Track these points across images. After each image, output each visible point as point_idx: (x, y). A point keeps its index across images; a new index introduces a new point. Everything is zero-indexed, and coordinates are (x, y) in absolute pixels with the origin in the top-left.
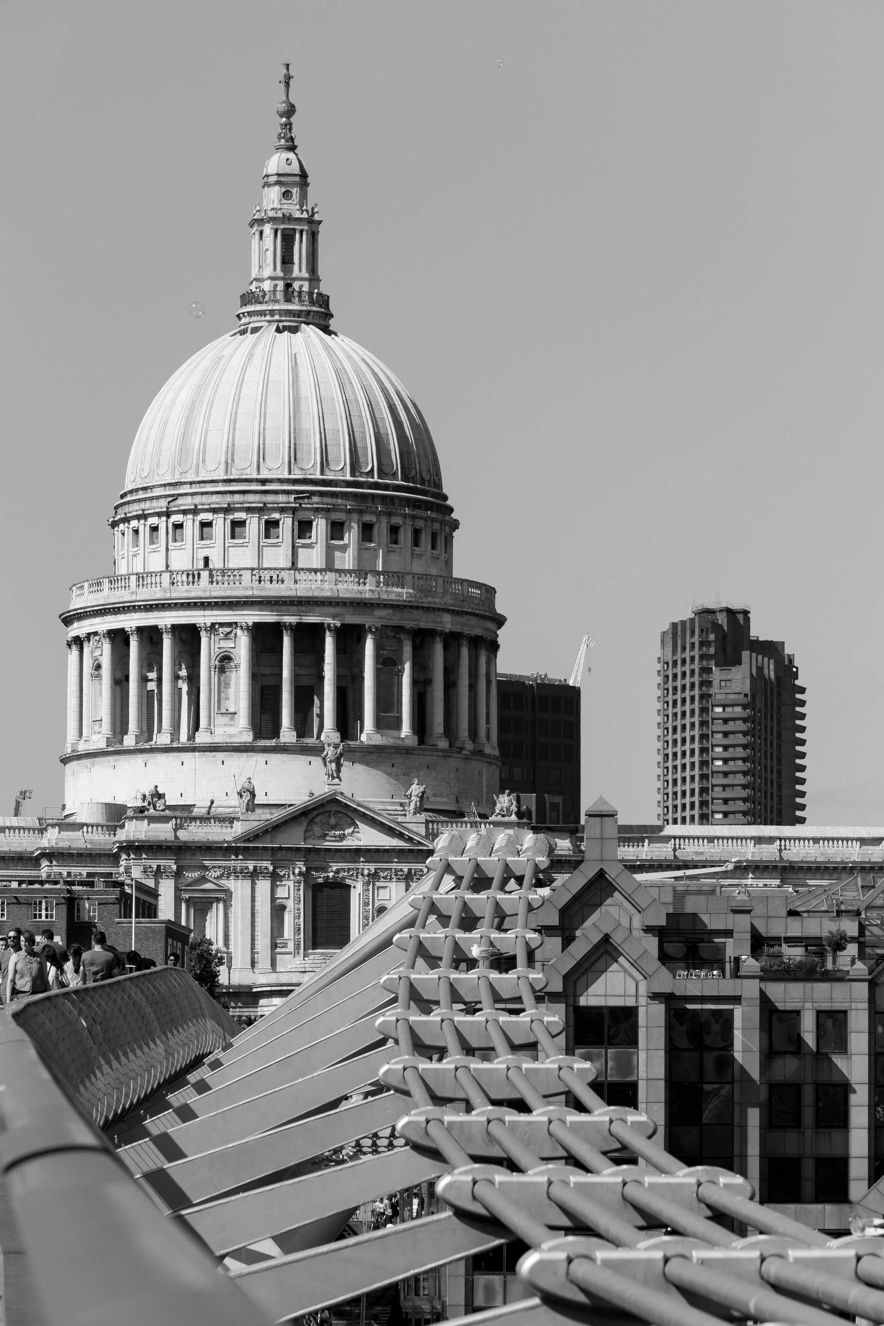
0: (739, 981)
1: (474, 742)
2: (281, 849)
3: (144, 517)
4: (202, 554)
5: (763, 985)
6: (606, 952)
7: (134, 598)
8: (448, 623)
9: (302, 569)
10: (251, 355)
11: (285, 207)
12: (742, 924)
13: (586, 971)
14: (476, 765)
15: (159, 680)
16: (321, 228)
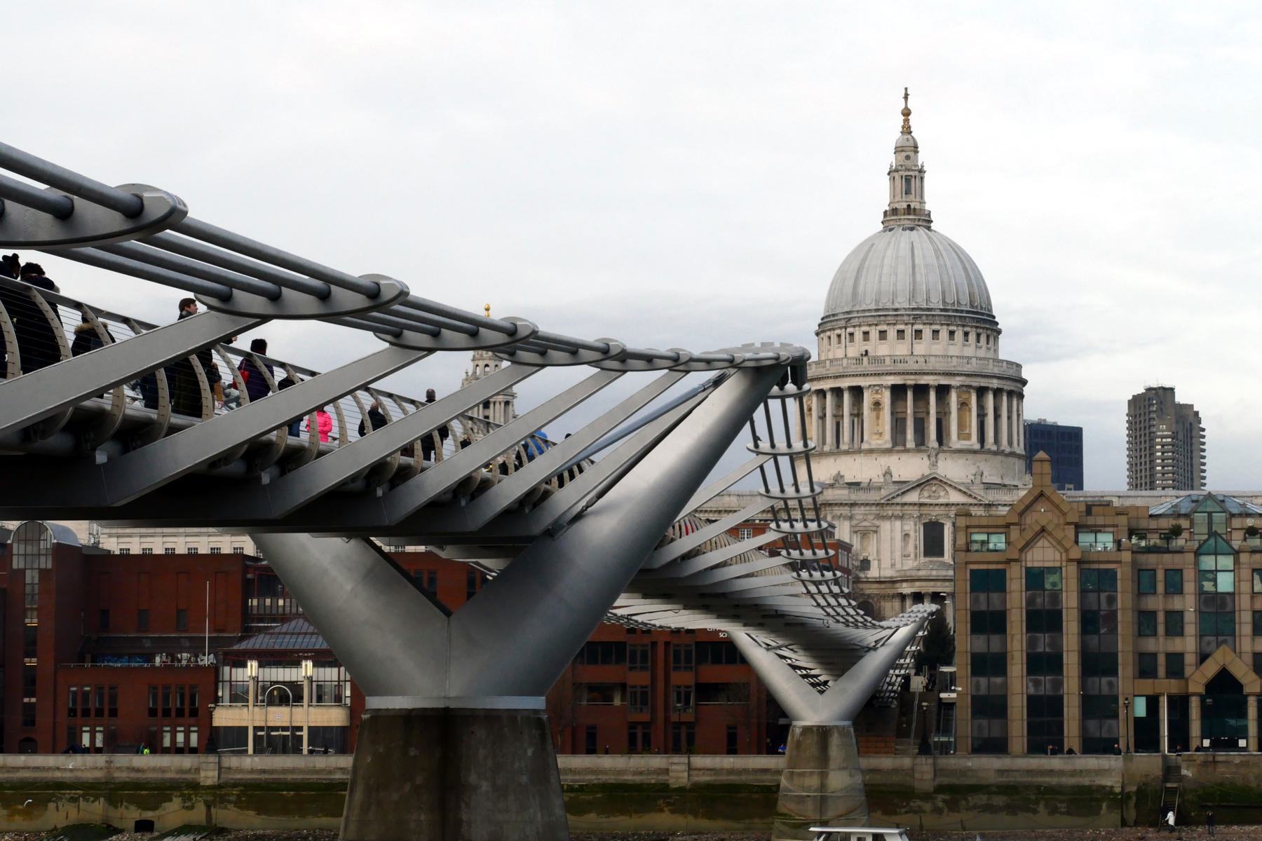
0: (1119, 552)
1: (1011, 447)
2: (906, 504)
3: (834, 329)
4: (863, 351)
5: (1134, 555)
6: (1043, 536)
7: (828, 372)
8: (995, 384)
9: (917, 355)
10: (889, 243)
11: (906, 163)
12: (1123, 520)
13: (1032, 547)
14: (1011, 460)
15: (843, 416)
16: (926, 176)
